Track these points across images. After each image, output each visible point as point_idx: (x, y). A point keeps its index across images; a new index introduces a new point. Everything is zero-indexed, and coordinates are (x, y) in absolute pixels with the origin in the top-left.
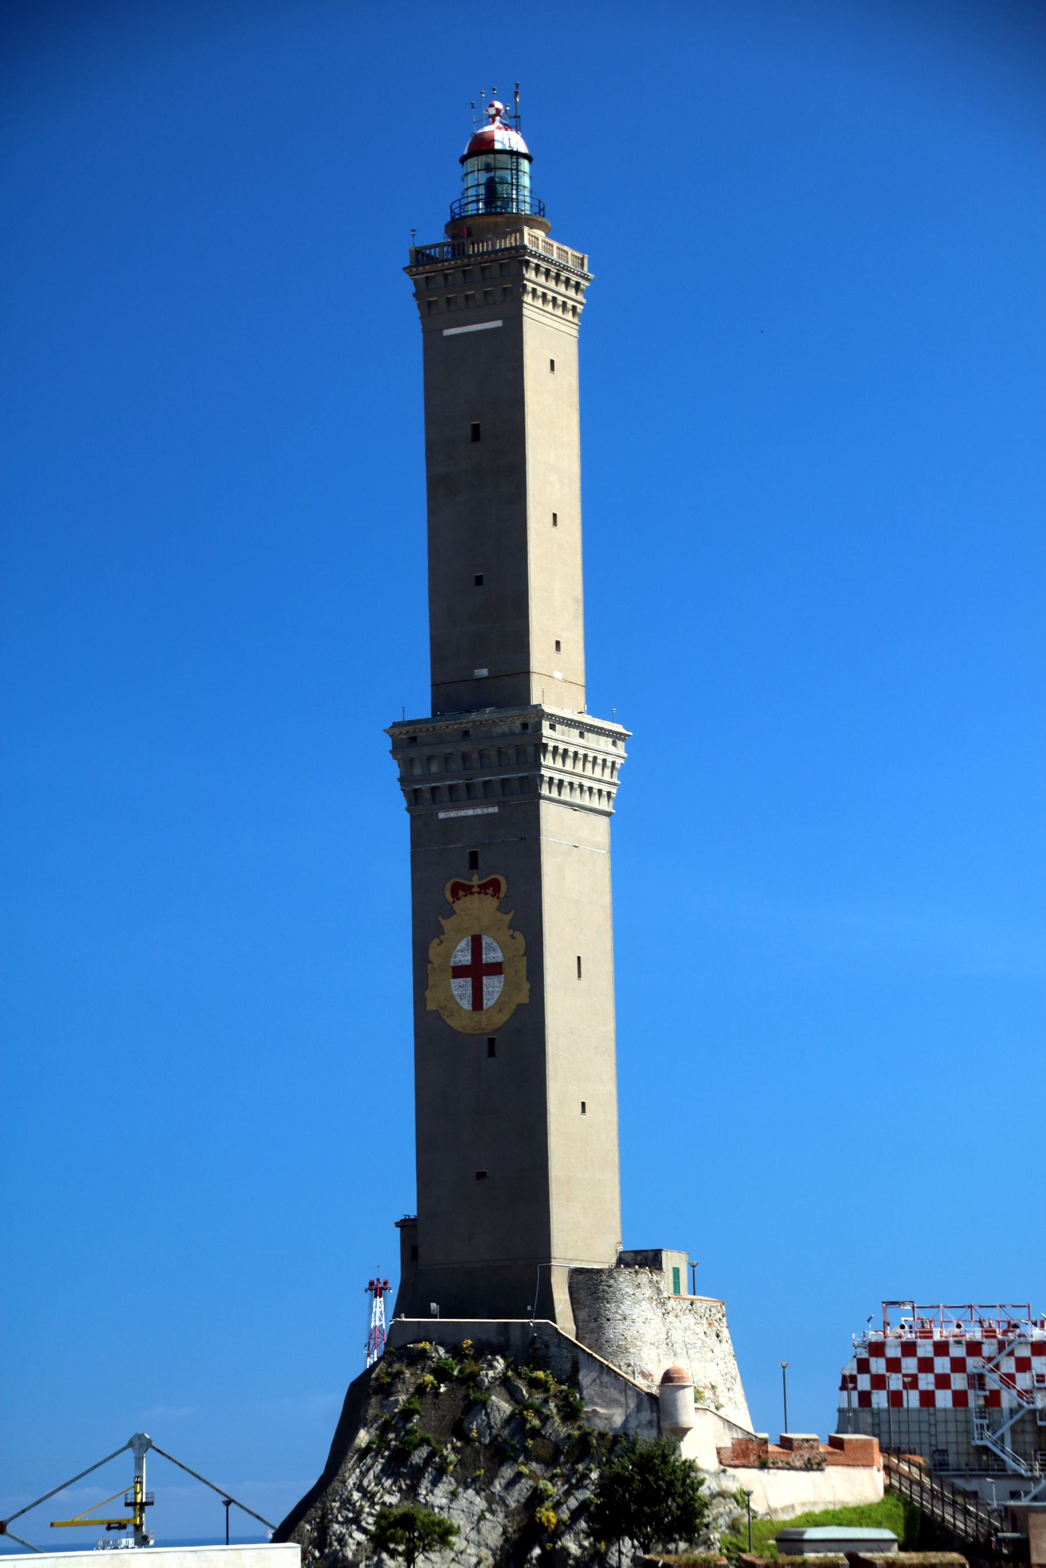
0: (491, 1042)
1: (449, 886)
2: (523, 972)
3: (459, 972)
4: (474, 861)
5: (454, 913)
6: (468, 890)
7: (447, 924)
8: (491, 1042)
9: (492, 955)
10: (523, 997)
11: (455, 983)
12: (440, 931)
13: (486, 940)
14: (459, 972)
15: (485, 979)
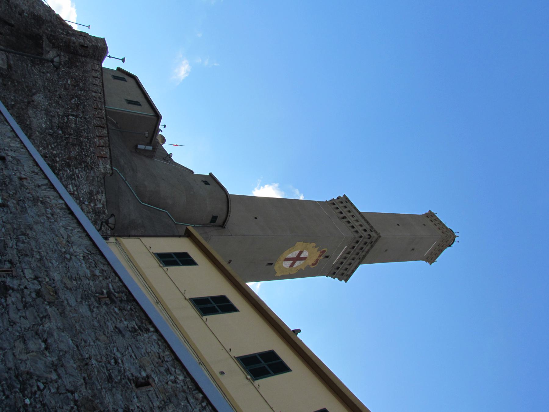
0: (271, 264)
1: (326, 249)
2: (285, 274)
3: (301, 253)
4: (327, 257)
5: (318, 251)
6: (320, 256)
7: (317, 249)
8: (271, 264)
9: (298, 264)
10: (278, 274)
11: (298, 252)
12: (316, 247)
13: (302, 261)
14: (301, 253)
15: (291, 262)
